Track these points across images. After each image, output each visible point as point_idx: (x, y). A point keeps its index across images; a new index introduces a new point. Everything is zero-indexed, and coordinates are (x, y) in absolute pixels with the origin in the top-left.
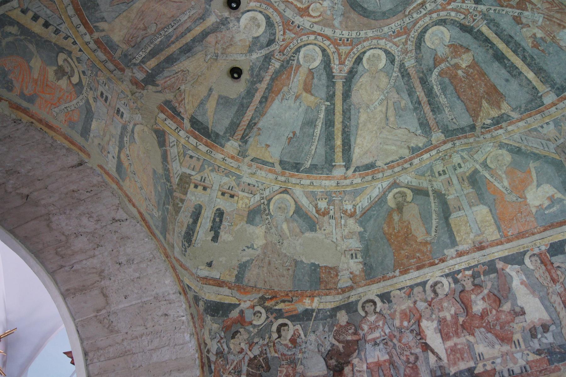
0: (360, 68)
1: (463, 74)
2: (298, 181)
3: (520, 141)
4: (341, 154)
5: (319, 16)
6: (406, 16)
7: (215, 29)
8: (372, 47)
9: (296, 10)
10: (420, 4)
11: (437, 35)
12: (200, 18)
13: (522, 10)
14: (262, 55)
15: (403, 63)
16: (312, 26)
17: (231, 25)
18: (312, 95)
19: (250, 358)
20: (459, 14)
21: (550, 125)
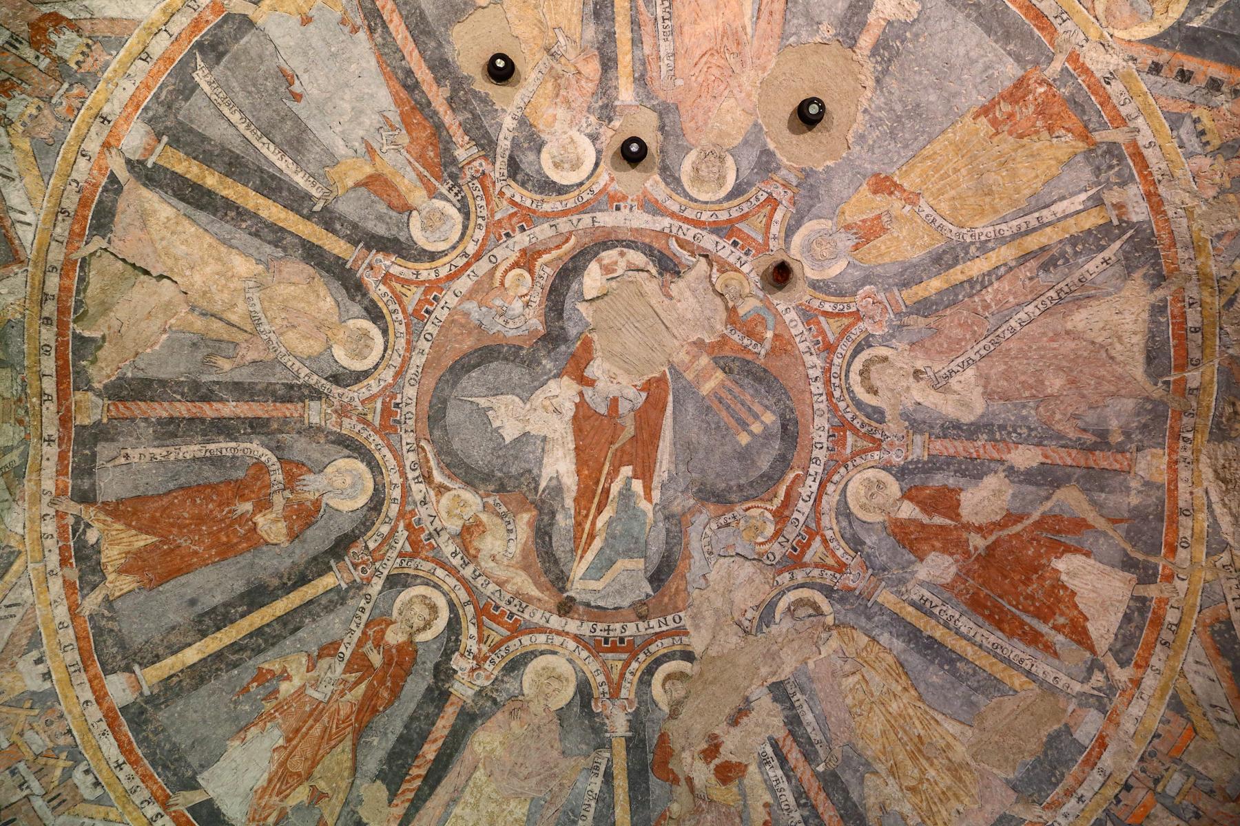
0: (356, 309)
1: (239, 512)
2: (175, 29)
3: (6, 602)
4: (179, 169)
5: (502, 284)
6: (418, 440)
7: (605, 87)
8: (389, 352)
9: (542, 248)
10: (430, 473)
11: (353, 485)
12: (642, 76)
13: (349, 661)
14: (501, 137)
15: (320, 399)
16: (493, 259)
17: (593, 119)
18: (358, 185)
20: (380, 540)
21: (40, 681)
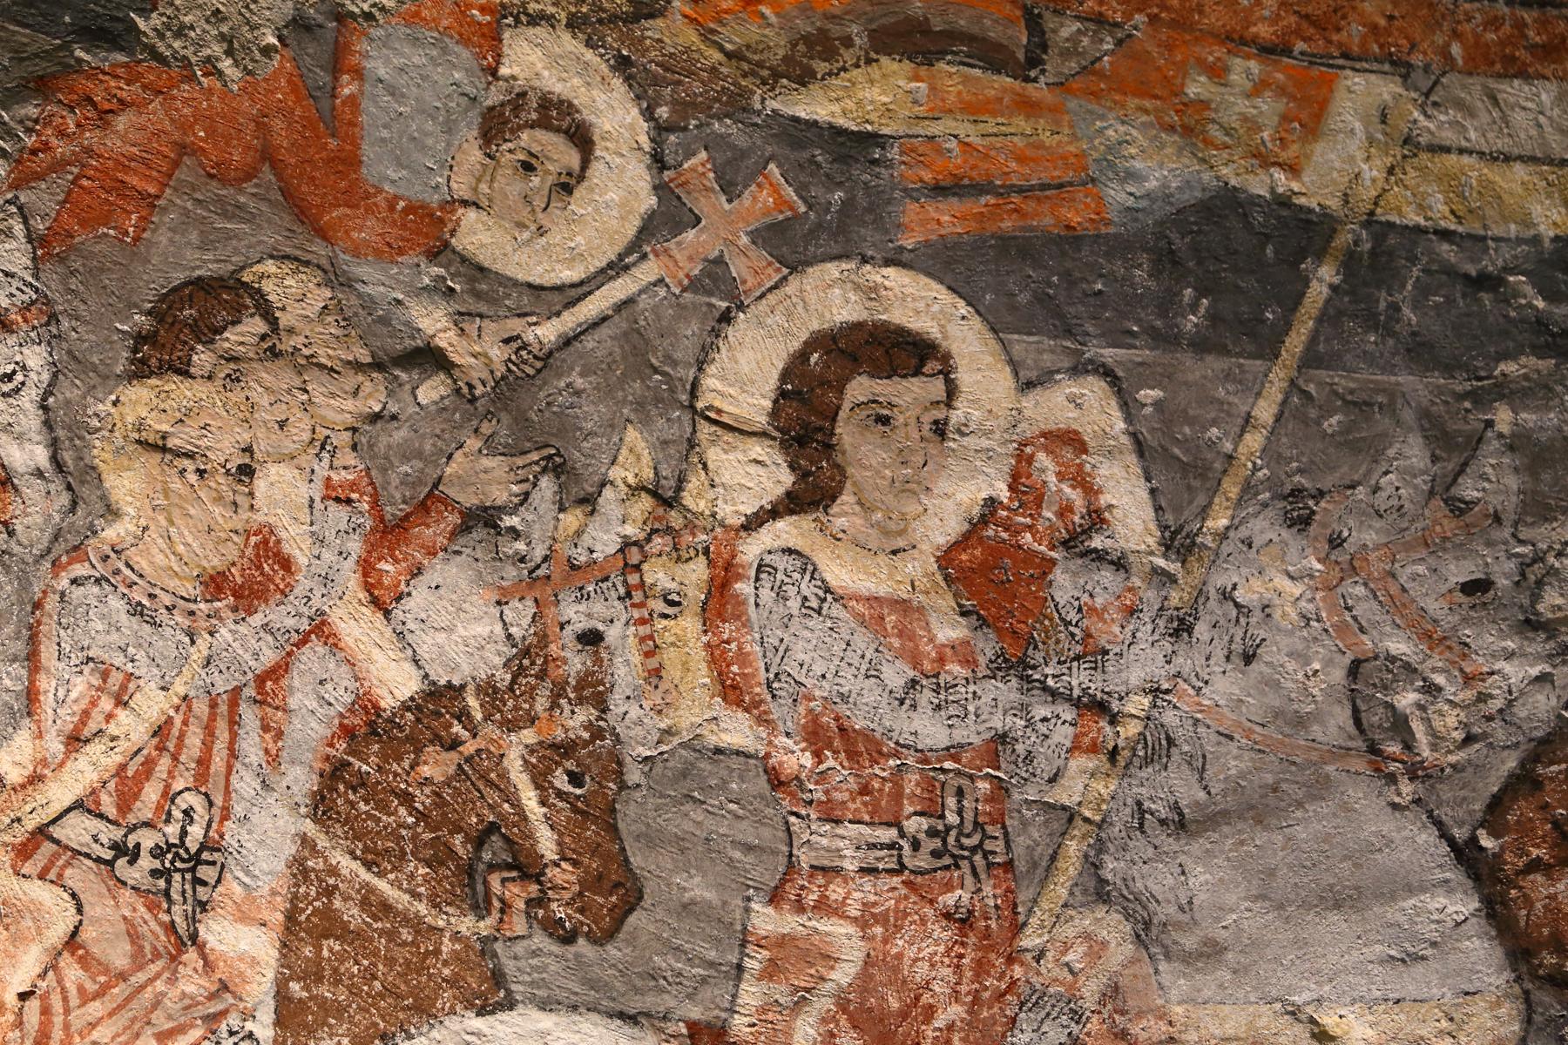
19: (366, 704)
